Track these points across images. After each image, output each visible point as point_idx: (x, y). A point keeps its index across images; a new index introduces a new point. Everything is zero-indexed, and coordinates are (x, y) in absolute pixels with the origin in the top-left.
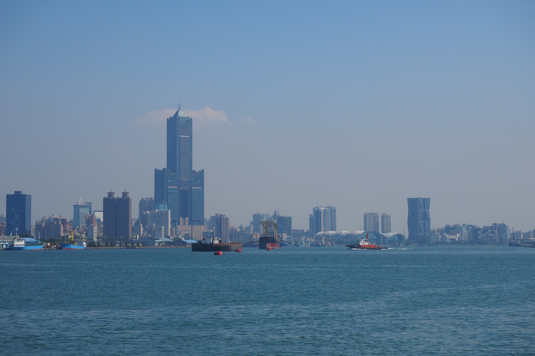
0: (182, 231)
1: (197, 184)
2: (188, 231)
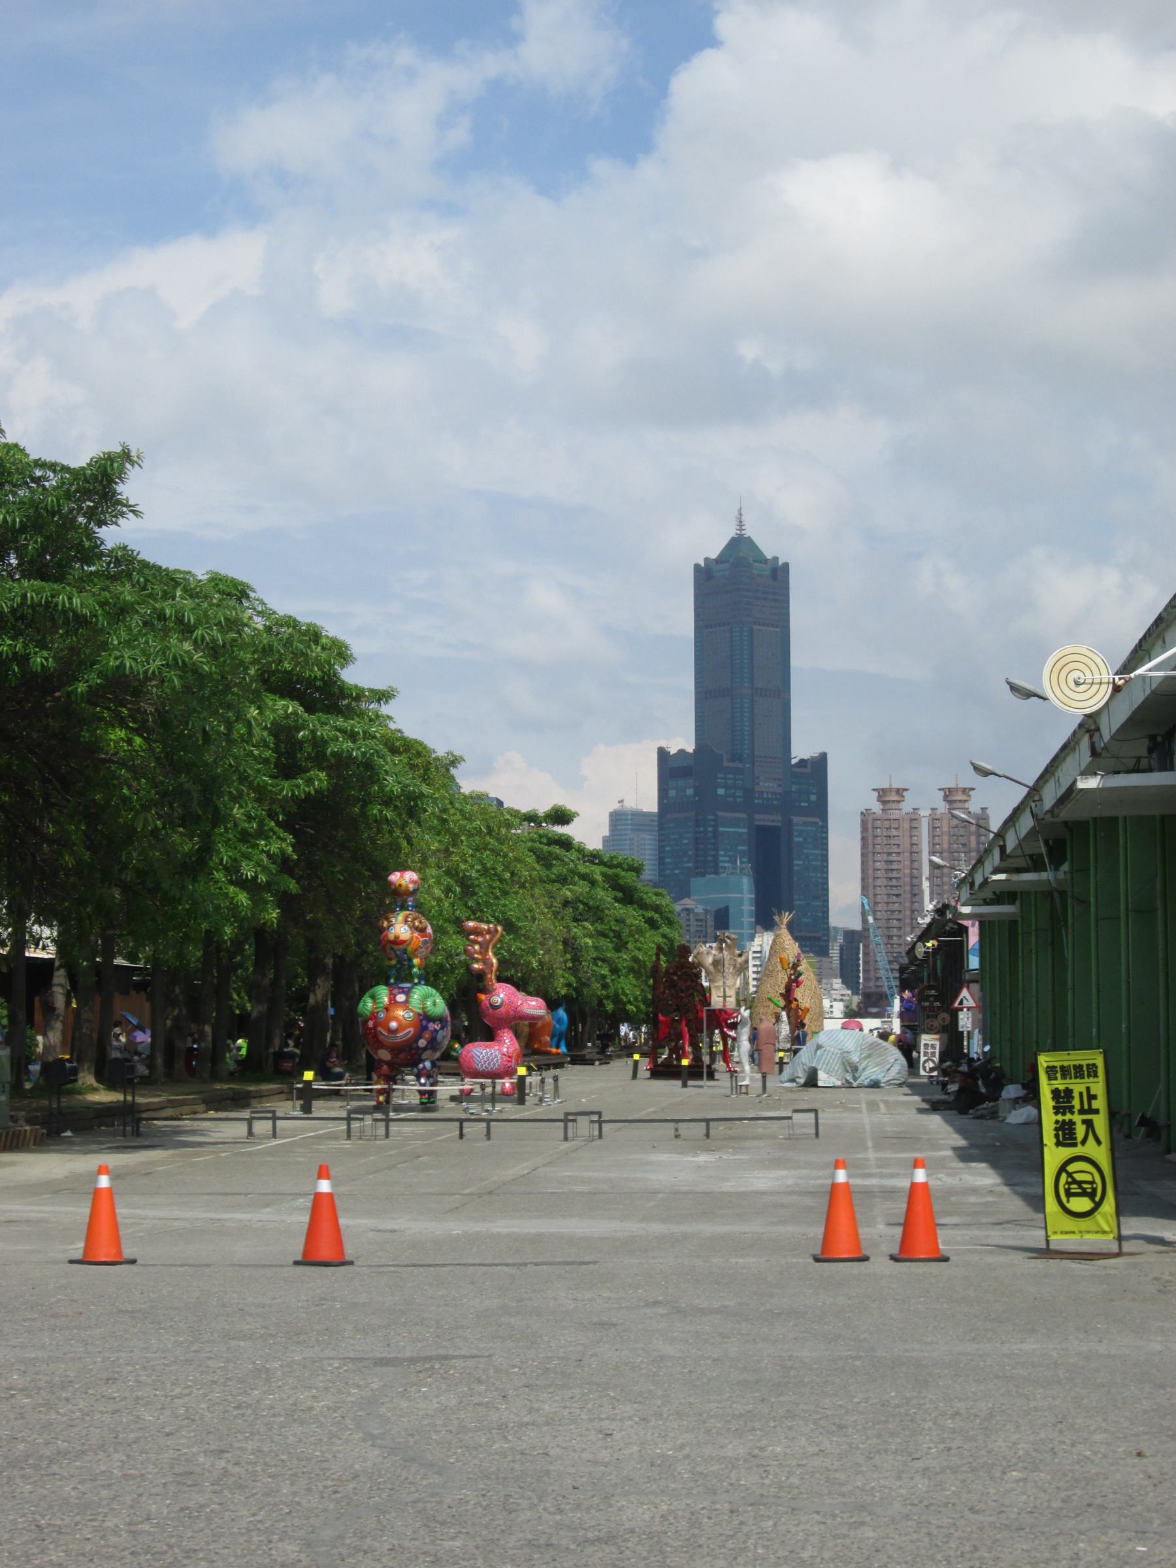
1: (806, 804)
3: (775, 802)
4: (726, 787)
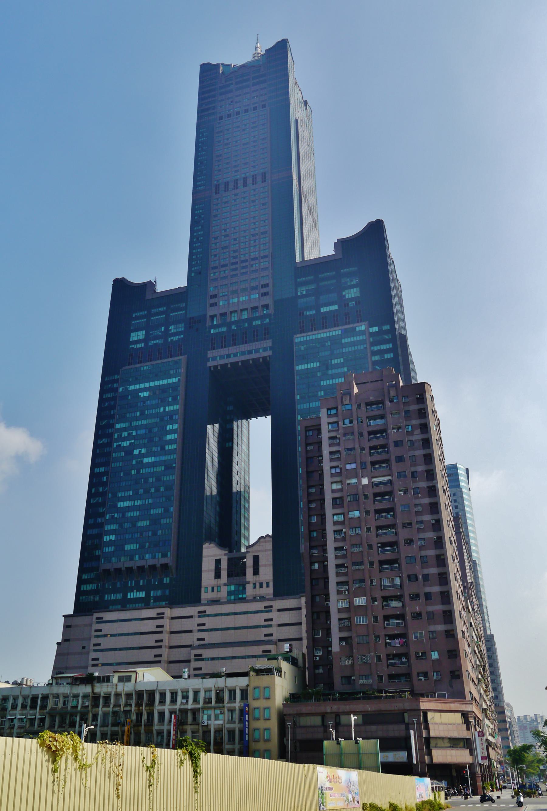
0: (207, 653)
1: (335, 307)
2: (258, 650)
3: (259, 322)
4: (148, 328)
